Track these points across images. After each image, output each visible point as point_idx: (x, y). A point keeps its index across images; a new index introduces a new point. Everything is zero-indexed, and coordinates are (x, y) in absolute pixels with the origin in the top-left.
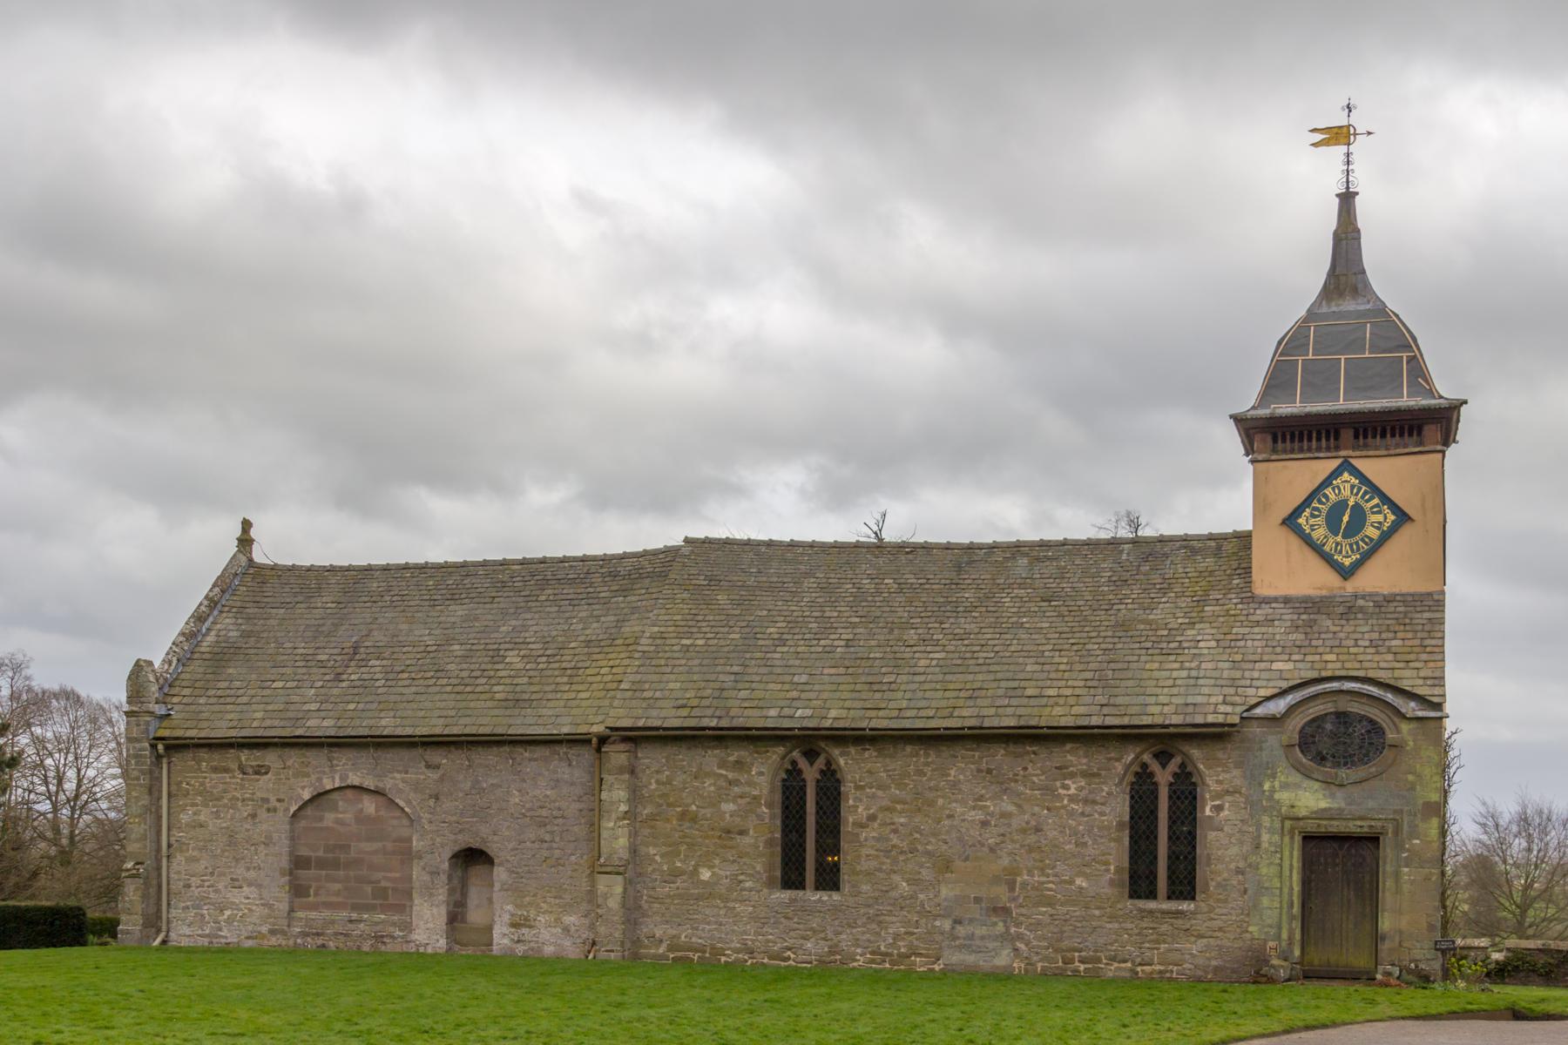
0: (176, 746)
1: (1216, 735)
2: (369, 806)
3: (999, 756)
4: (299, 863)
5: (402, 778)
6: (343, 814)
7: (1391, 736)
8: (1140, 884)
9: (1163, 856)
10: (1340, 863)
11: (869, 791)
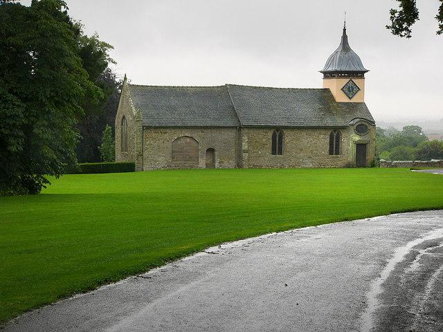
0: (149, 128)
1: (344, 128)
2: (188, 140)
3: (310, 132)
4: (173, 152)
5: (197, 135)
6: (182, 141)
7: (369, 128)
8: (331, 153)
9: (335, 148)
10: (361, 148)
11: (288, 138)
